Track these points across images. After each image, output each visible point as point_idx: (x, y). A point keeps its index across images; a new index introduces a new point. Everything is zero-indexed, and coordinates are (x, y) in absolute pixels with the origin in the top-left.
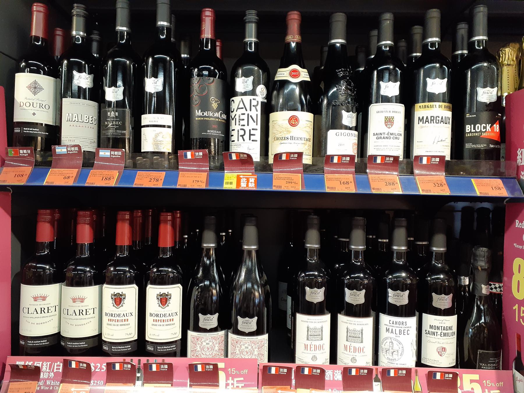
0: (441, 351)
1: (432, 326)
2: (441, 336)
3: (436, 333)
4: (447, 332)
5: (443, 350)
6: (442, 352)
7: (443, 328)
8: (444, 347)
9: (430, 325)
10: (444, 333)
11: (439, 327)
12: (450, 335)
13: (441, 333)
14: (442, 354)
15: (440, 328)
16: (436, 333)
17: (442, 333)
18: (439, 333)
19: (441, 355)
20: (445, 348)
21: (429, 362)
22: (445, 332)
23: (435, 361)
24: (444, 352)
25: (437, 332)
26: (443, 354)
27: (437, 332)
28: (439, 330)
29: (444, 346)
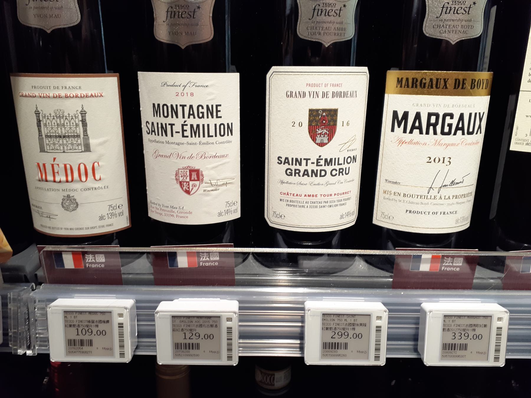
0: (188, 180)
1: (159, 105)
2: (183, 136)
3: (169, 127)
4: (201, 122)
5: (194, 176)
6: (191, 183)
7: (187, 109)
8: (197, 168)
9: (154, 105)
10: (192, 126)
11: (177, 106)
12: (212, 133)
13: (183, 125)
14: (191, 188)
15: (180, 109)
16: (169, 127)
17: (185, 128)
18: (177, 128)
19: (188, 192)
20: (197, 171)
21: (161, 212)
22: (195, 121)
23: (174, 210)
24: (197, 183)
25: (172, 125)
26: (195, 189)
27: (172, 125)
28: (177, 117)
29: (196, 164)
